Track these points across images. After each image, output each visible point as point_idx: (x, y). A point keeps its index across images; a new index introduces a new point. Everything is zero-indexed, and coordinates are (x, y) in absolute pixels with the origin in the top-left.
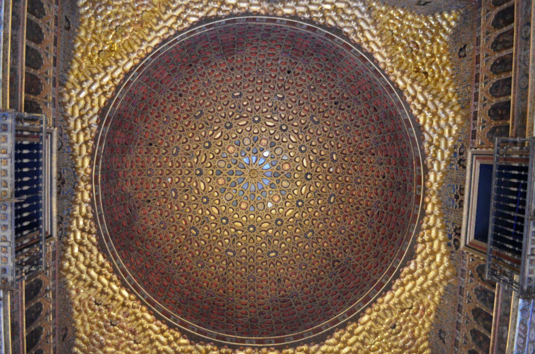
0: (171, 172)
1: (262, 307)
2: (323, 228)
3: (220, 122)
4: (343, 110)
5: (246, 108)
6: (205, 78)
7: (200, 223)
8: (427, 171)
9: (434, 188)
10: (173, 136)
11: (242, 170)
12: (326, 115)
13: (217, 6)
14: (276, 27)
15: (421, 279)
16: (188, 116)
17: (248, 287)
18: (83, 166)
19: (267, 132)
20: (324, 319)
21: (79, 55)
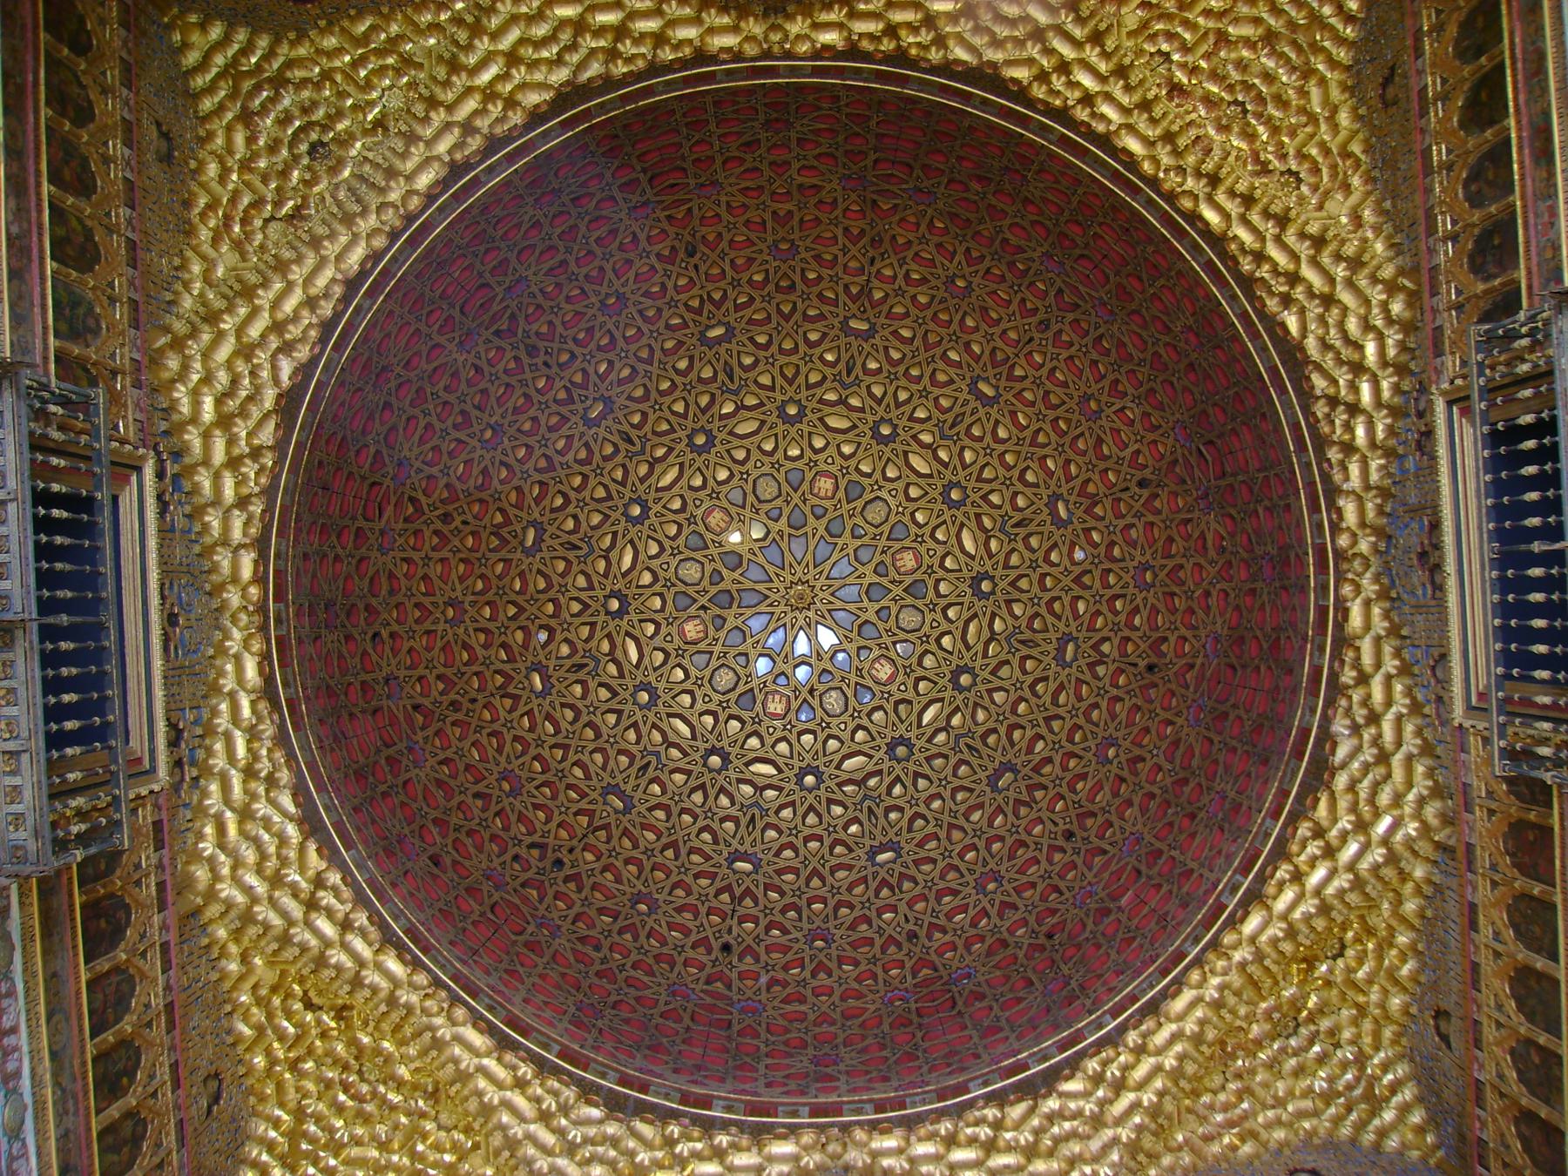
0: (1077, 580)
1: (748, 165)
2: (554, 436)
3: (928, 759)
4: (532, 846)
5: (851, 814)
6: (999, 898)
7: (968, 420)
8: (268, 691)
9: (237, 635)
10: (1080, 699)
11: (839, 604)
12: (584, 820)
13: (1008, 1135)
14: (803, 1093)
15: (254, 332)
16: (1036, 770)
17: (795, 222)
18: (1367, 604)
19: (769, 741)
20: (549, 155)
21: (1402, 939)
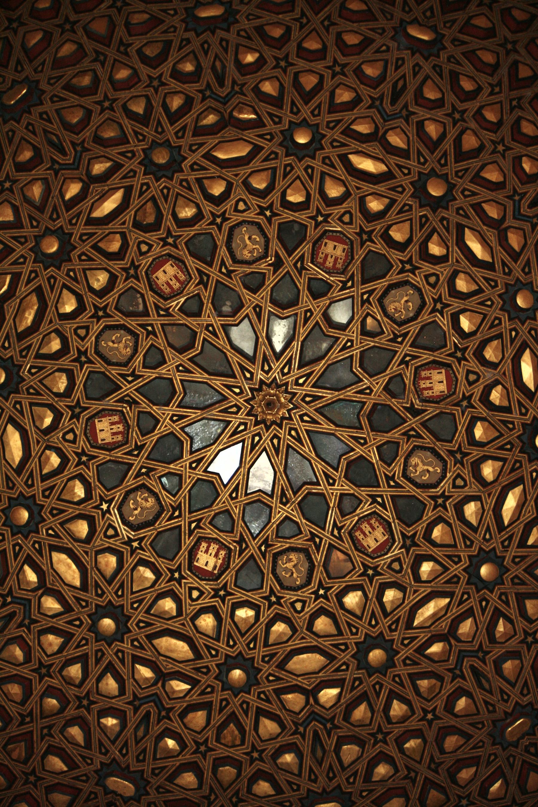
3: (123, 140)
5: (251, 80)
11: (217, 382)
19: (351, 204)
